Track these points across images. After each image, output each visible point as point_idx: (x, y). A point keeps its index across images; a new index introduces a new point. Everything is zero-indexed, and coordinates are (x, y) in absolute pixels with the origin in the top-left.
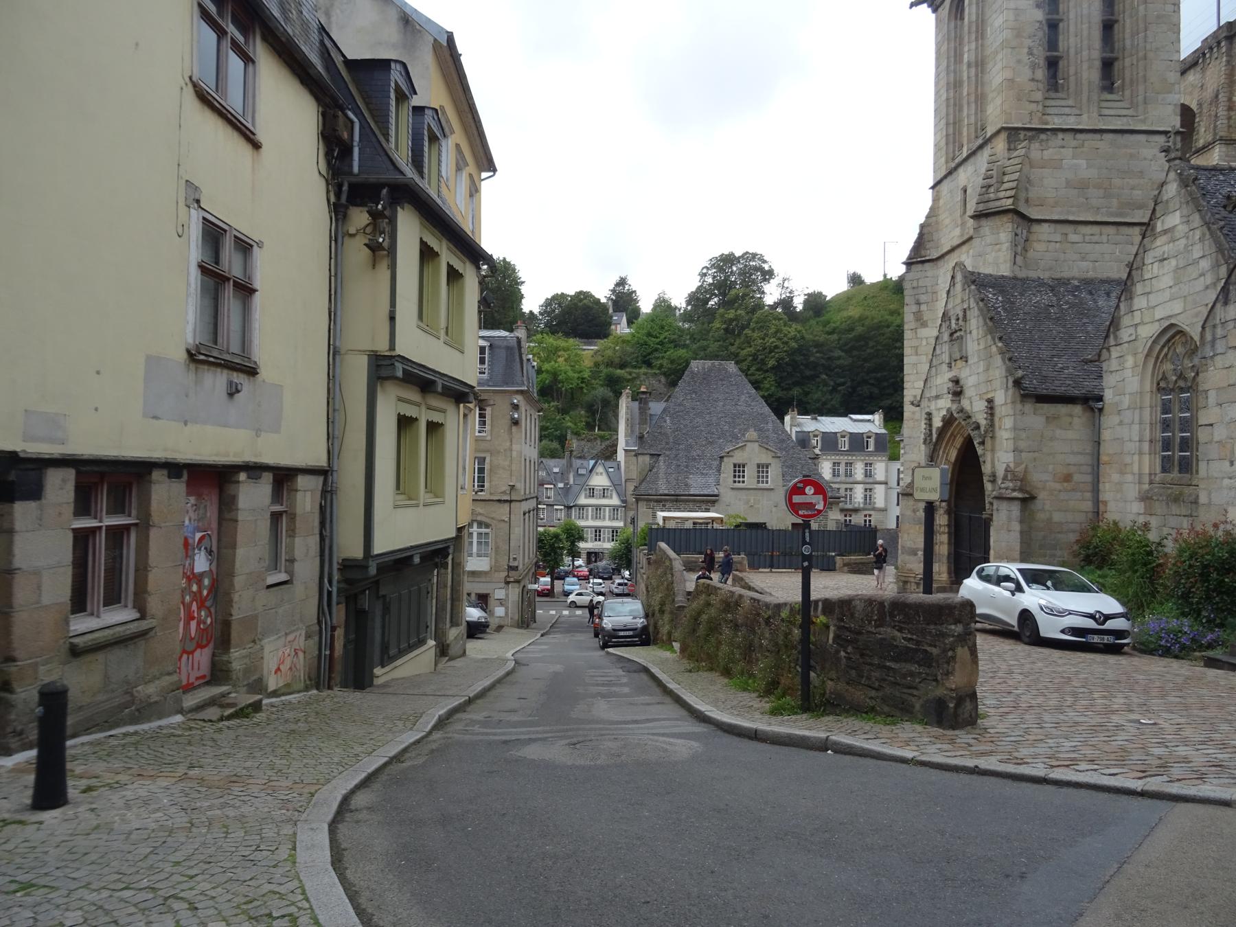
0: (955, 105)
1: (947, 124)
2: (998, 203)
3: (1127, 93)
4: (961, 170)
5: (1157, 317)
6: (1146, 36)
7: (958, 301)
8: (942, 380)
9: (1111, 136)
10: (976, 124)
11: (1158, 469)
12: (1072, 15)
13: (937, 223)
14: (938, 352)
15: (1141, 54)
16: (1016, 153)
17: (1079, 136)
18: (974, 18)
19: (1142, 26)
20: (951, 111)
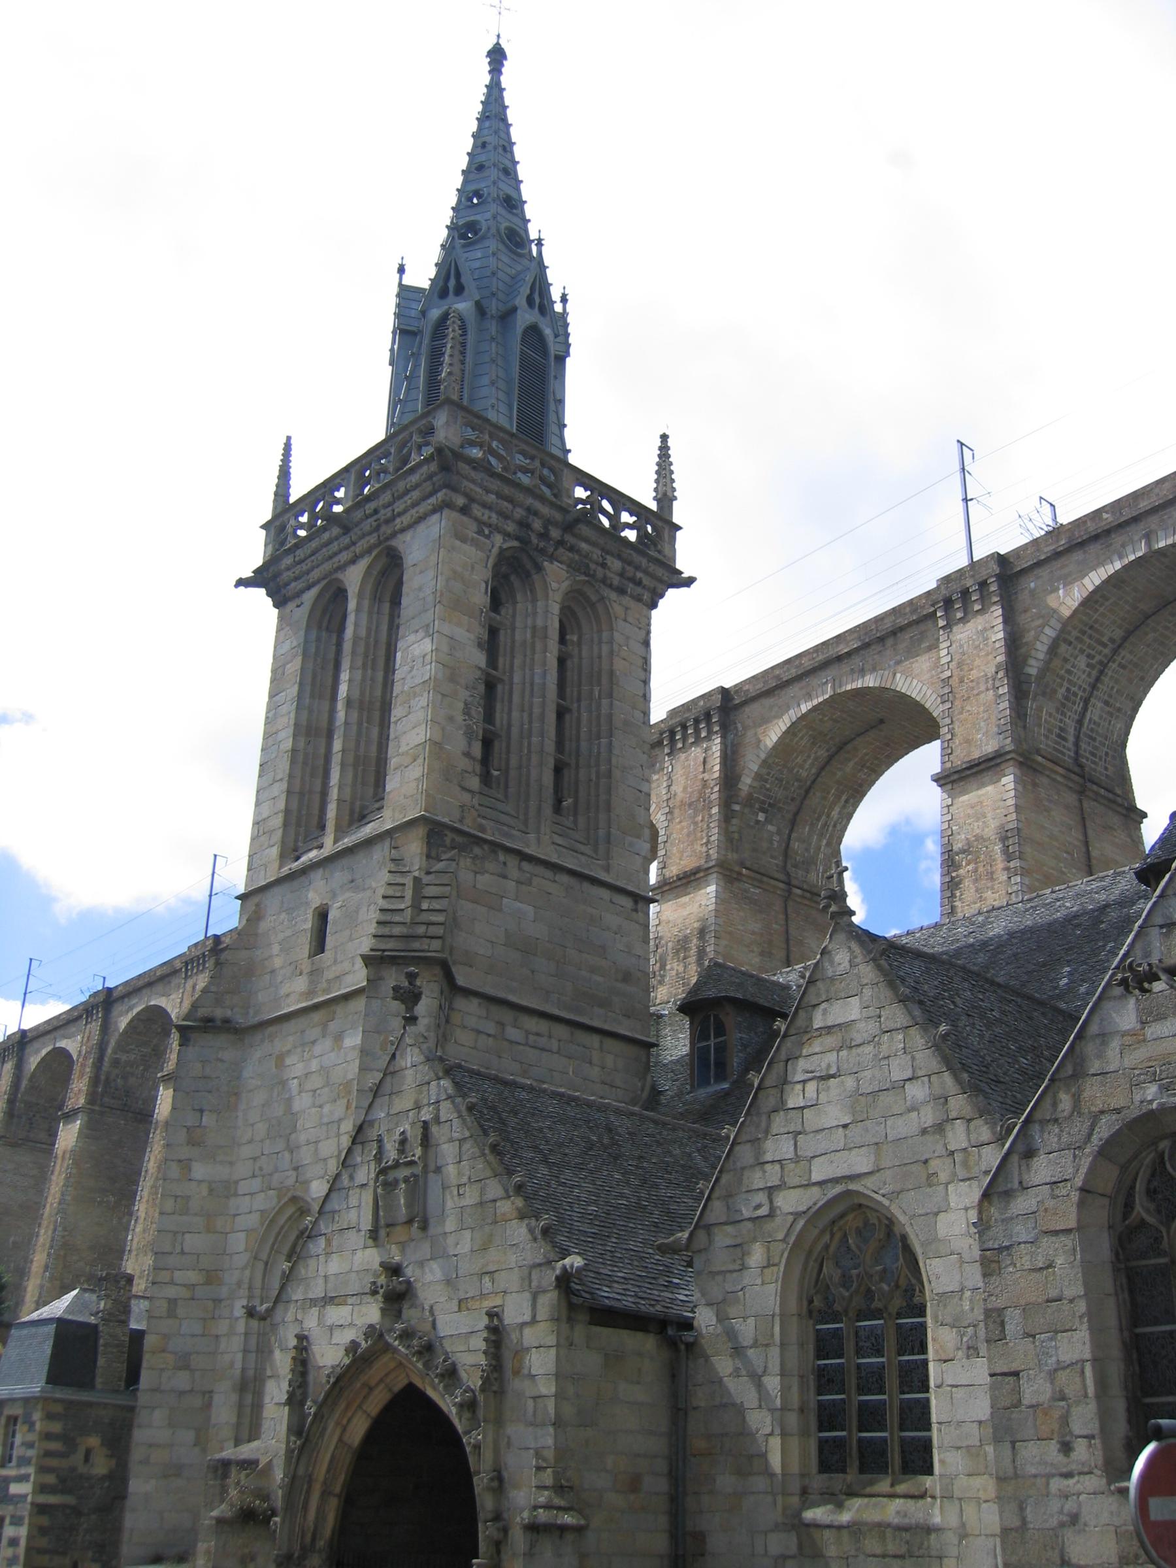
0: (305, 763)
2: (416, 945)
3: (582, 820)
4: (317, 876)
5: (816, 1177)
6: (610, 743)
9: (564, 878)
11: (814, 1468)
12: (517, 679)
16: (440, 866)
17: (526, 865)
18: (363, 633)
19: (604, 728)
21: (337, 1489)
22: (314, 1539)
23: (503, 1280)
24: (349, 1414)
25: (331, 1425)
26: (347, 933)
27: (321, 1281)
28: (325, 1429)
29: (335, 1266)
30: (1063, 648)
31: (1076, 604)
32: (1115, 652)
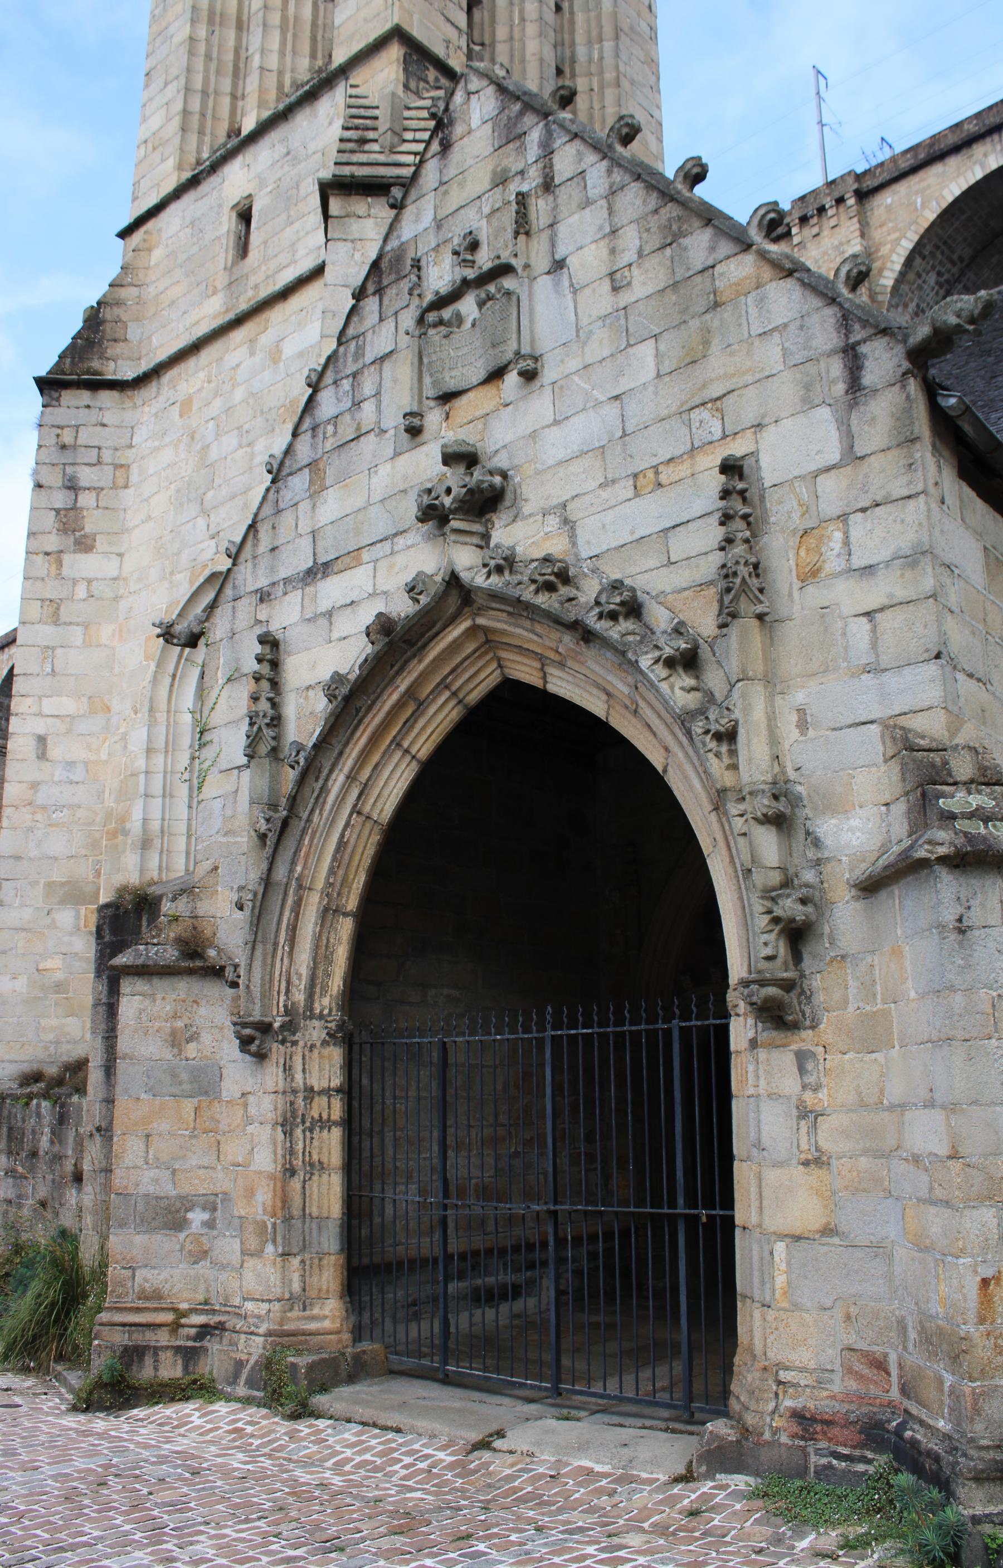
0: (208, 57)
1: (188, 90)
7: (480, 179)
8: (392, 473)
10: (281, 73)
13: (139, 301)
14: (328, 404)
15: (609, 76)
20: (199, 64)
21: (352, 903)
22: (310, 996)
23: (745, 408)
24: (375, 759)
25: (339, 779)
27: (306, 543)
28: (324, 790)
29: (332, 506)
30: (918, 261)
31: (935, 216)
32: (962, 272)
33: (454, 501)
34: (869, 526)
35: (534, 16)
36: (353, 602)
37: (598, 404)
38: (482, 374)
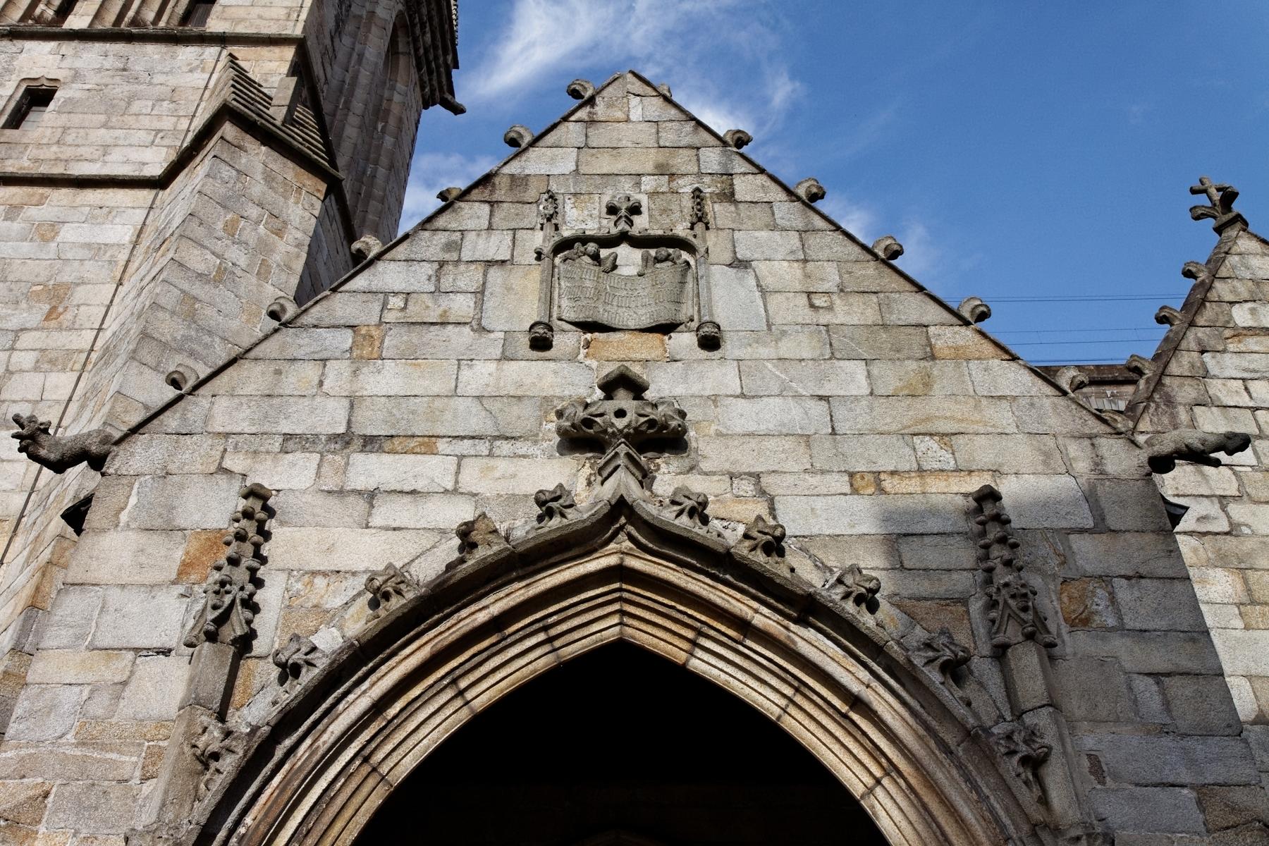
26: (102, 118)
33: (628, 426)
34: (1137, 594)
35: (358, 112)
36: (413, 492)
37: (798, 396)
38: (646, 322)
